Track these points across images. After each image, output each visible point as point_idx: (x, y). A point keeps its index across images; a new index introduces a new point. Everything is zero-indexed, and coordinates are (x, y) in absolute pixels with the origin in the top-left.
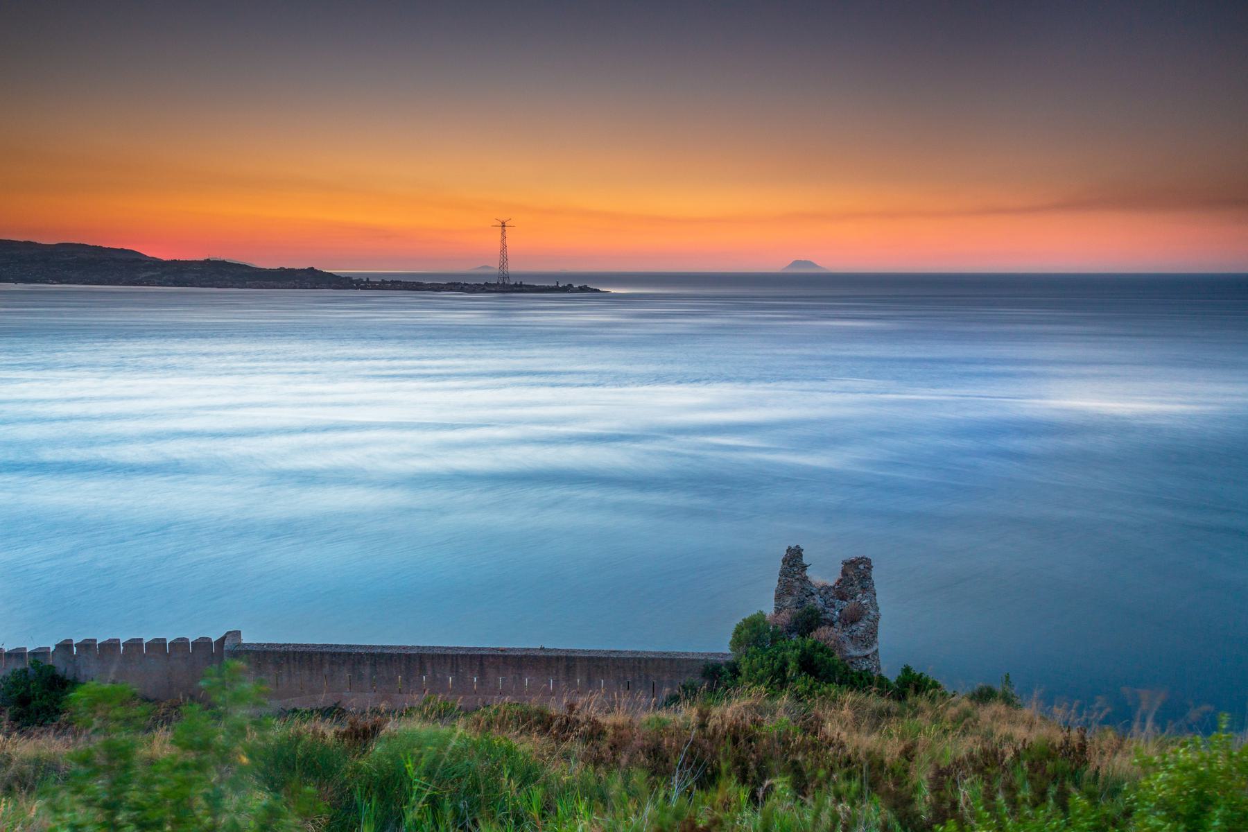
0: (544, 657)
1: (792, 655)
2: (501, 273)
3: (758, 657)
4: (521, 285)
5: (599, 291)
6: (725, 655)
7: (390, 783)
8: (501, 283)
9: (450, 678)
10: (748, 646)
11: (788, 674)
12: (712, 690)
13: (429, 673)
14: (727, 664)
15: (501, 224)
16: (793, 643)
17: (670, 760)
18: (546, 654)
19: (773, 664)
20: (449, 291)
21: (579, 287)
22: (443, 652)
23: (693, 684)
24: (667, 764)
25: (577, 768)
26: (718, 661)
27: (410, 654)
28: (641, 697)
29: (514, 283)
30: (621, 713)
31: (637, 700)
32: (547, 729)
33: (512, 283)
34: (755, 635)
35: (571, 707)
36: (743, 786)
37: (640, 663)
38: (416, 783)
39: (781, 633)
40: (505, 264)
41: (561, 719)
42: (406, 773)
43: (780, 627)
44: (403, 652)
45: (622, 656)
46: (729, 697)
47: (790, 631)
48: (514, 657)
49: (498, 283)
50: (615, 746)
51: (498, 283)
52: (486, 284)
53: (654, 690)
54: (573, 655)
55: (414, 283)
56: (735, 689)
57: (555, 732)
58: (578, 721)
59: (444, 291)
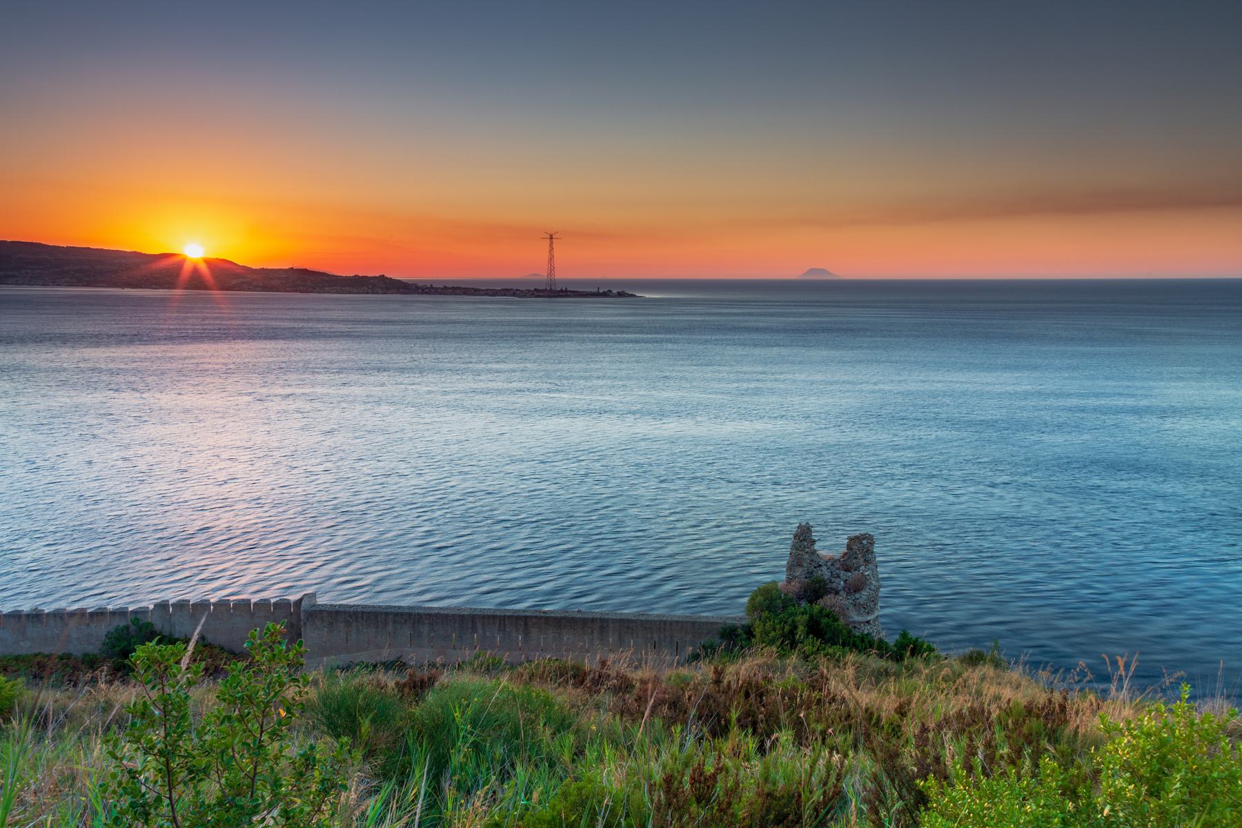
0: (581, 618)
1: (802, 620)
3: (770, 621)
4: (566, 291)
5: (635, 296)
10: (762, 611)
11: (797, 637)
12: (729, 650)
13: (480, 631)
14: (743, 627)
16: (802, 610)
19: (784, 627)
22: (492, 614)
32: (582, 683)
34: (768, 602)
35: (603, 663)
39: (791, 600)
43: (790, 595)
44: (458, 612)
46: (744, 656)
47: (800, 598)
53: (678, 649)
54: (606, 617)
56: (749, 649)
58: (609, 676)
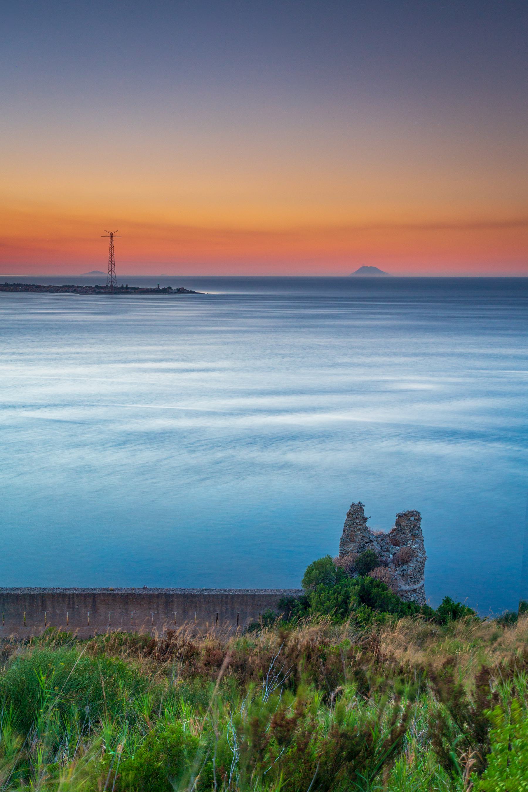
0: (147, 595)
1: (354, 591)
2: (110, 277)
3: (325, 592)
4: (127, 288)
5: (194, 292)
6: (298, 591)
7: (24, 694)
8: (109, 285)
9: (68, 613)
10: (317, 583)
11: (350, 606)
12: (286, 619)
13: (50, 609)
14: (300, 598)
15: (109, 235)
16: (354, 581)
17: (254, 673)
18: (149, 593)
19: (337, 598)
20: (63, 292)
21: (177, 289)
22: (61, 593)
23: (271, 614)
24: (252, 676)
25: (178, 681)
26: (292, 596)
27: (34, 595)
28: (228, 626)
29: (121, 286)
30: (211, 638)
31: (225, 628)
32: (150, 652)
33: (119, 286)
34: (323, 575)
35: (171, 634)
36: (317, 691)
37: (227, 598)
38: (47, 693)
39: (344, 572)
40: (113, 269)
41: (162, 643)
42: (38, 684)
43: (344, 568)
44: (28, 592)
45: (212, 593)
46: (301, 625)
47: (352, 571)
48: (122, 595)
49: (107, 286)
50: (209, 663)
51: (107, 286)
52: (97, 287)
53: (238, 620)
54: (171, 593)
55: (34, 285)
56: (306, 618)
57: (157, 654)
58: (175, 645)
59: (60, 292)
